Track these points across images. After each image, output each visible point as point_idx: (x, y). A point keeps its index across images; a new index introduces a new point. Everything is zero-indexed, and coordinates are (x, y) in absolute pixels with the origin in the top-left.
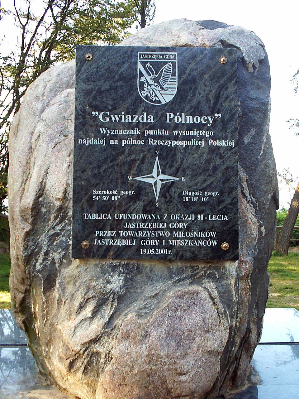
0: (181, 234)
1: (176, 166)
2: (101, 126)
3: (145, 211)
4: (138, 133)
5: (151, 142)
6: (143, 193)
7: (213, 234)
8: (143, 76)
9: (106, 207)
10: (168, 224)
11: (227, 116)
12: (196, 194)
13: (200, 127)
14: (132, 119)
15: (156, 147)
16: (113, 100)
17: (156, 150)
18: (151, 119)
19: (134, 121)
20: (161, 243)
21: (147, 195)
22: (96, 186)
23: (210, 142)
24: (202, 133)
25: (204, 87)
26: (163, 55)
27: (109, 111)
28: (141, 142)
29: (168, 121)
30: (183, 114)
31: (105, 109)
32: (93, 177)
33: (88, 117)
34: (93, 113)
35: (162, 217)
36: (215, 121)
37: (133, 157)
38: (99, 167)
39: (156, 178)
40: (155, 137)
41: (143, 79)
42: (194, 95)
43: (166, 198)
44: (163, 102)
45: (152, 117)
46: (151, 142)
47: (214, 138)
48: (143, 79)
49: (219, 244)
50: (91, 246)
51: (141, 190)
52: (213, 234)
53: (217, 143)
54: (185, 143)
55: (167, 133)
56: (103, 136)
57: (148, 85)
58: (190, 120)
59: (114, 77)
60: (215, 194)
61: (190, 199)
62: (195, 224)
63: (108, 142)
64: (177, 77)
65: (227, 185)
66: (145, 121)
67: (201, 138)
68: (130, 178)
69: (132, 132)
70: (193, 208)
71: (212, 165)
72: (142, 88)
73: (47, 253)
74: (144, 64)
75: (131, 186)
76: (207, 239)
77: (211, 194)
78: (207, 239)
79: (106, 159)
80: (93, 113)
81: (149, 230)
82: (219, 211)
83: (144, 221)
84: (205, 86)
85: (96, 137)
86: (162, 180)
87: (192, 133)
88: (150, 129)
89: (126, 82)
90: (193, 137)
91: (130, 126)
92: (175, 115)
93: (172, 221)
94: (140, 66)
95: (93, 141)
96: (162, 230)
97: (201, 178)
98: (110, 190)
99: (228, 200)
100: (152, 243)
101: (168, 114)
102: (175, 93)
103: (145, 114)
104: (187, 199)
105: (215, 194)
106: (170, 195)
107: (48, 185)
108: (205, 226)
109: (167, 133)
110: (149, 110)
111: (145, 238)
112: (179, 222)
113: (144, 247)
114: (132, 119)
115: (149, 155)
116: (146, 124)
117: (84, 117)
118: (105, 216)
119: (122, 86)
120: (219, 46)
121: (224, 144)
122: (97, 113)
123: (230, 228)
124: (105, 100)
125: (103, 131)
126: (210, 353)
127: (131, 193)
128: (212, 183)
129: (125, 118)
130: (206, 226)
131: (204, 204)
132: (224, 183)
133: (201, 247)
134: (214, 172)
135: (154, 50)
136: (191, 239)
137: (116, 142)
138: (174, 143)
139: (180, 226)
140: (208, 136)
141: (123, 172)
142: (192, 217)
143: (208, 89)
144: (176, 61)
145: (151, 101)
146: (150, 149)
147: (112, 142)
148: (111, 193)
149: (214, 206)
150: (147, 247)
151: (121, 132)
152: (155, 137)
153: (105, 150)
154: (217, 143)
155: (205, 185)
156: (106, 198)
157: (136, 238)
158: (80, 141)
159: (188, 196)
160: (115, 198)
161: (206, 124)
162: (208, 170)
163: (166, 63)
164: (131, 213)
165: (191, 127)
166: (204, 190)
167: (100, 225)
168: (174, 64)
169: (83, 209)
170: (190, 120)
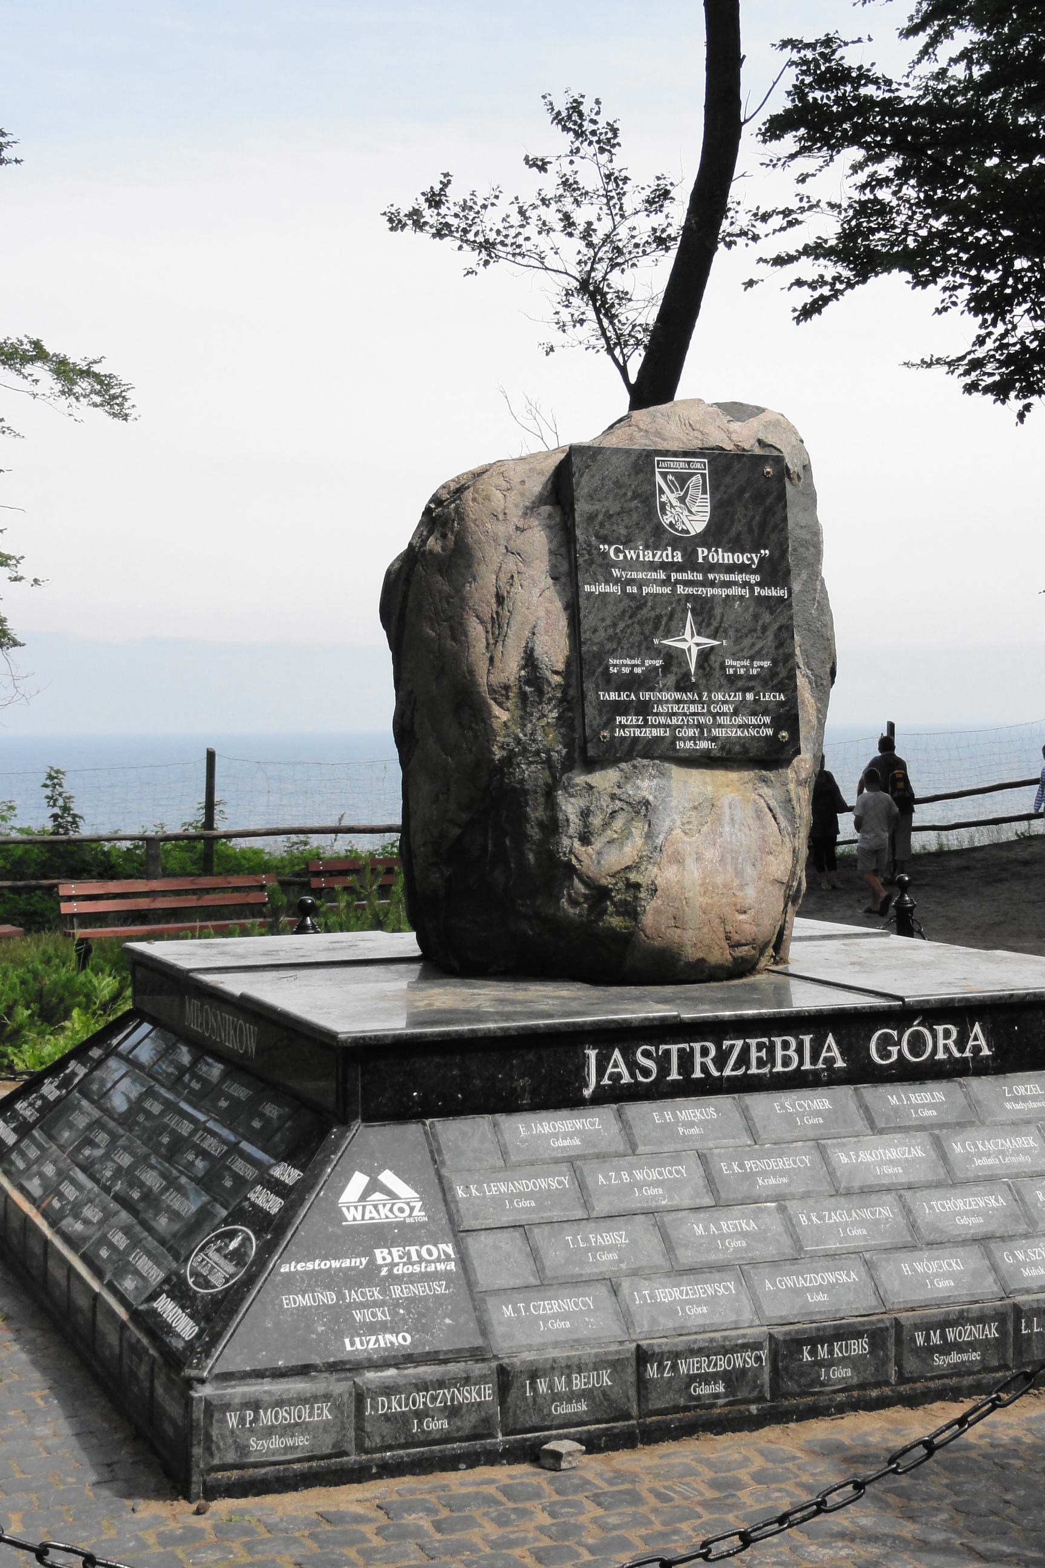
1: (715, 624)
2: (613, 566)
3: (679, 688)
4: (663, 577)
5: (680, 589)
6: (675, 662)
7: (767, 720)
8: (664, 493)
9: (631, 683)
10: (709, 707)
11: (777, 554)
12: (742, 663)
13: (742, 568)
14: (654, 556)
15: (688, 597)
16: (626, 527)
17: (687, 601)
18: (678, 558)
19: (656, 559)
20: (702, 732)
21: (680, 665)
22: (612, 653)
23: (757, 589)
25: (744, 511)
26: (689, 463)
27: (623, 544)
28: (667, 590)
29: (700, 560)
30: (720, 550)
31: (618, 541)
32: (608, 640)
33: (595, 552)
34: (601, 546)
35: (700, 696)
36: (762, 559)
37: (658, 611)
38: (615, 625)
39: (690, 642)
40: (687, 583)
41: (664, 499)
42: (733, 521)
43: (704, 669)
44: (693, 533)
45: (679, 554)
49: (776, 733)
50: (613, 737)
51: (673, 659)
52: (767, 720)
53: (766, 592)
54: (723, 592)
56: (617, 581)
57: (672, 506)
58: (728, 558)
59: (625, 494)
60: (766, 664)
61: (735, 672)
62: (744, 706)
63: (624, 590)
64: (708, 496)
65: (781, 651)
66: (670, 560)
67: (745, 584)
68: (656, 641)
69: (653, 575)
70: (740, 684)
71: (760, 623)
72: (664, 512)
74: (664, 475)
75: (657, 652)
76: (759, 726)
77: (762, 663)
78: (759, 726)
79: (624, 612)
80: (601, 546)
81: (685, 714)
82: (773, 687)
83: (678, 702)
84: (746, 508)
85: (607, 582)
86: (698, 644)
87: (732, 577)
88: (677, 571)
89: (642, 502)
90: (735, 583)
91: (652, 566)
92: (710, 551)
93: (714, 702)
94: (659, 479)
95: (603, 588)
96: (703, 714)
97: (747, 642)
98: (632, 658)
99: (783, 673)
100: (690, 732)
101: (700, 550)
102: (707, 519)
103: (669, 549)
104: (731, 672)
105: (766, 664)
106: (709, 666)
107: (539, 651)
110: (676, 543)
111: (681, 727)
112: (724, 702)
113: (680, 739)
114: (654, 556)
115: (679, 609)
116: (673, 564)
117: (589, 553)
118: (628, 696)
119: (637, 508)
120: (758, 451)
121: (774, 594)
122: (606, 547)
123: (788, 711)
124: (615, 527)
125: (616, 572)
127: (658, 663)
128: (762, 648)
129: (644, 556)
130: (758, 708)
131: (752, 678)
132: (777, 648)
133: (753, 738)
134: (763, 633)
135: (675, 454)
136: (740, 726)
137: (635, 591)
138: (711, 591)
139: (725, 708)
140: (753, 582)
141: (647, 632)
143: (750, 513)
144: (706, 472)
145: (676, 530)
146: (680, 600)
147: (629, 589)
148: (633, 662)
152: (687, 583)
153: (621, 601)
154: (766, 592)
155: (752, 652)
157: (669, 726)
159: (733, 667)
160: (638, 670)
161: (750, 565)
162: (755, 630)
164: (661, 691)
165: (731, 569)
166: (752, 659)
167: (621, 708)
168: (703, 476)
169: (597, 686)
170: (728, 558)
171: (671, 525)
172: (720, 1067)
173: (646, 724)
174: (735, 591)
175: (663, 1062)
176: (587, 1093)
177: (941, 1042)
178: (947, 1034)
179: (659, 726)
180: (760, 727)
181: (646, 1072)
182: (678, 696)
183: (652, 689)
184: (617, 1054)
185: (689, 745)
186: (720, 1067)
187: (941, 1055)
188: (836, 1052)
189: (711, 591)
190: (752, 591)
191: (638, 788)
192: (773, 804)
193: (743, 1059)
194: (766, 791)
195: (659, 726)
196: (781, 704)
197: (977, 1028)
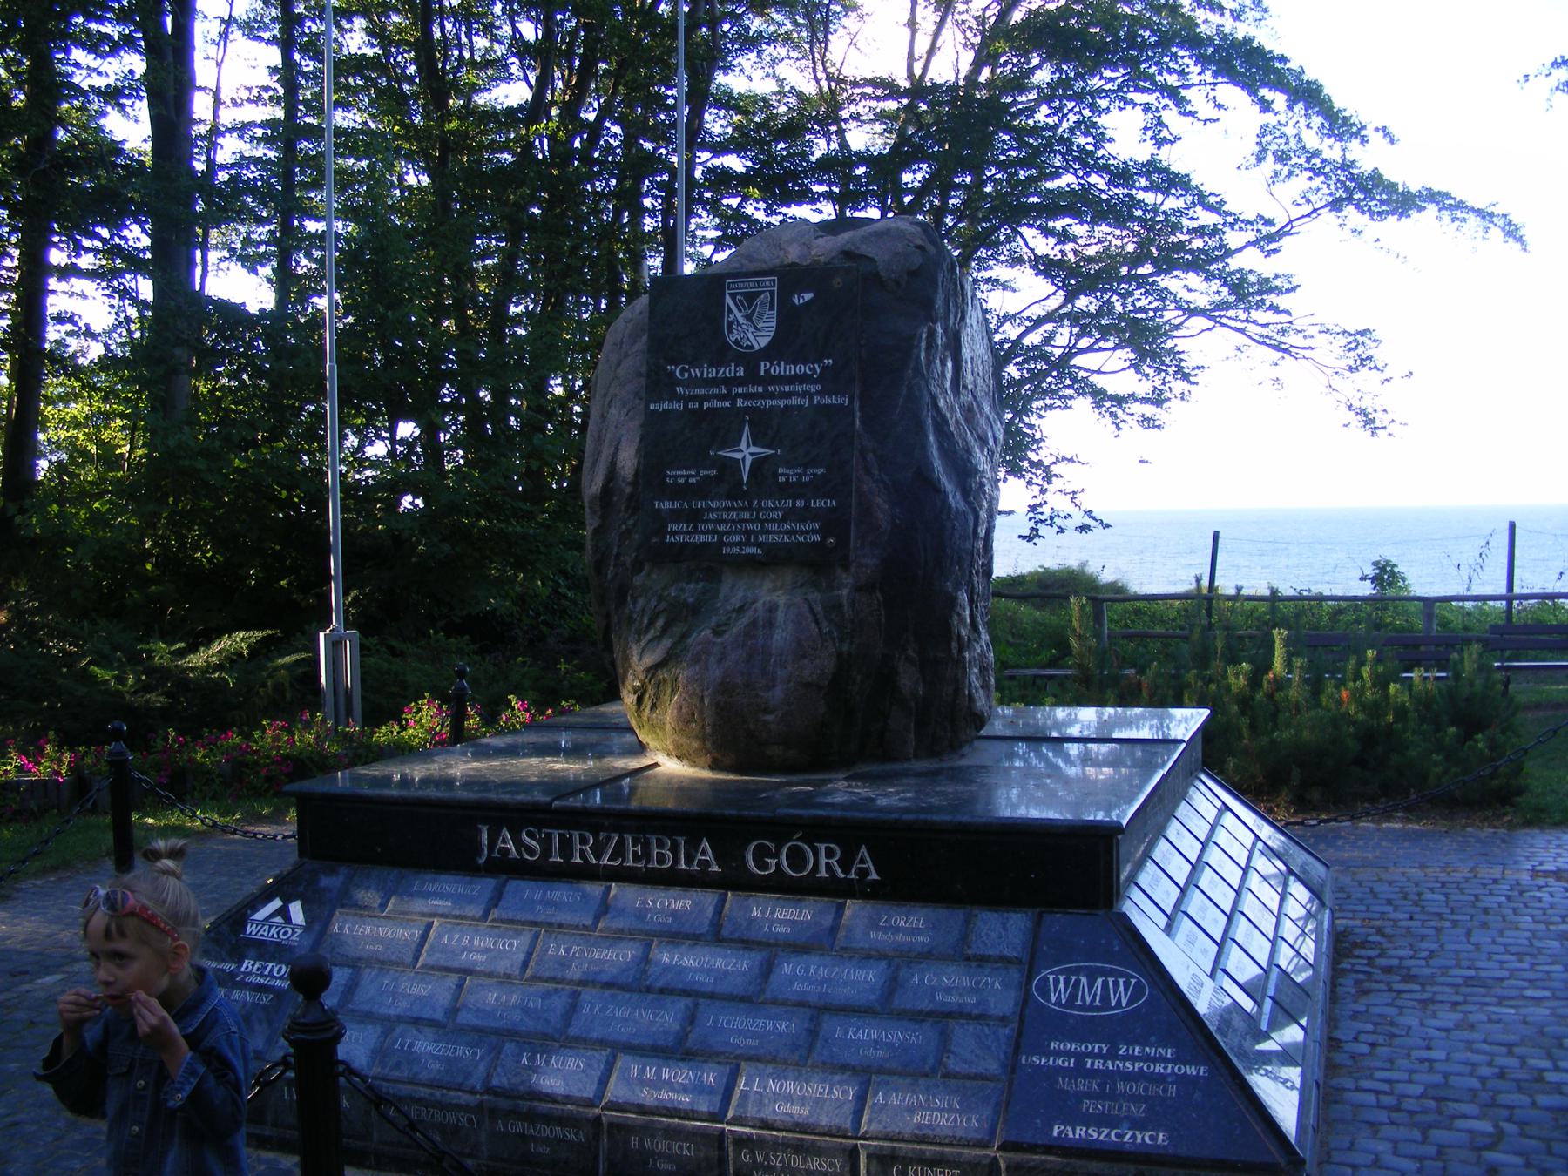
0: (774, 527)
3: (730, 497)
9: (678, 492)
15: (746, 410)
20: (748, 539)
24: (806, 387)
28: (728, 404)
35: (750, 503)
36: (824, 369)
40: (746, 396)
41: (732, 318)
44: (757, 347)
46: (739, 403)
47: (820, 393)
48: (732, 318)
49: (824, 539)
50: (663, 542)
52: (816, 526)
54: (782, 403)
55: (761, 390)
58: (791, 370)
60: (819, 471)
63: (686, 406)
67: (804, 394)
69: (716, 391)
72: (730, 331)
73: (618, 556)
74: (733, 296)
76: (807, 532)
83: (728, 509)
85: (671, 401)
87: (793, 388)
88: (738, 385)
94: (728, 299)
95: (666, 406)
96: (751, 521)
100: (737, 539)
105: (819, 471)
108: (804, 515)
109: (761, 390)
111: (728, 533)
112: (773, 510)
125: (680, 390)
126: (807, 685)
133: (800, 543)
138: (769, 403)
139: (774, 515)
142: (790, 503)
147: (690, 405)
149: (817, 488)
150: (730, 545)
151: (704, 391)
152: (746, 396)
154: (825, 401)
156: (681, 481)
158: (652, 407)
163: (761, 293)
165: (791, 380)
166: (805, 466)
168: (772, 293)
170: (791, 370)
171: (737, 342)
172: (598, 856)
173: (696, 531)
174: (788, 402)
175: (546, 844)
176: (482, 861)
177: (824, 860)
178: (830, 854)
179: (708, 532)
180: (809, 533)
181: (531, 851)
182: (729, 504)
183: (704, 497)
184: (506, 833)
185: (735, 550)
186: (598, 856)
187: (823, 874)
188: (710, 857)
189: (769, 403)
190: (811, 400)
191: (683, 590)
192: (818, 608)
193: (619, 852)
194: (815, 596)
195: (708, 532)
196: (832, 509)
197: (863, 850)
